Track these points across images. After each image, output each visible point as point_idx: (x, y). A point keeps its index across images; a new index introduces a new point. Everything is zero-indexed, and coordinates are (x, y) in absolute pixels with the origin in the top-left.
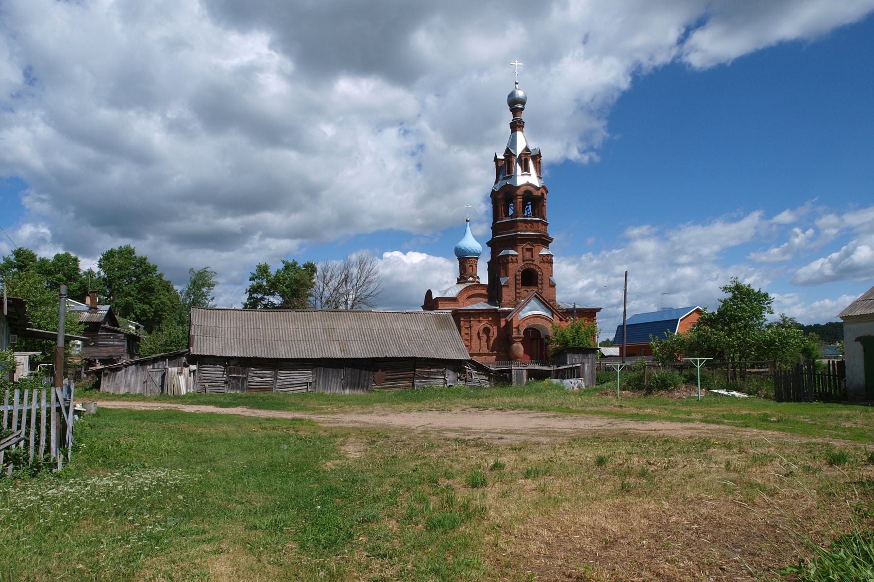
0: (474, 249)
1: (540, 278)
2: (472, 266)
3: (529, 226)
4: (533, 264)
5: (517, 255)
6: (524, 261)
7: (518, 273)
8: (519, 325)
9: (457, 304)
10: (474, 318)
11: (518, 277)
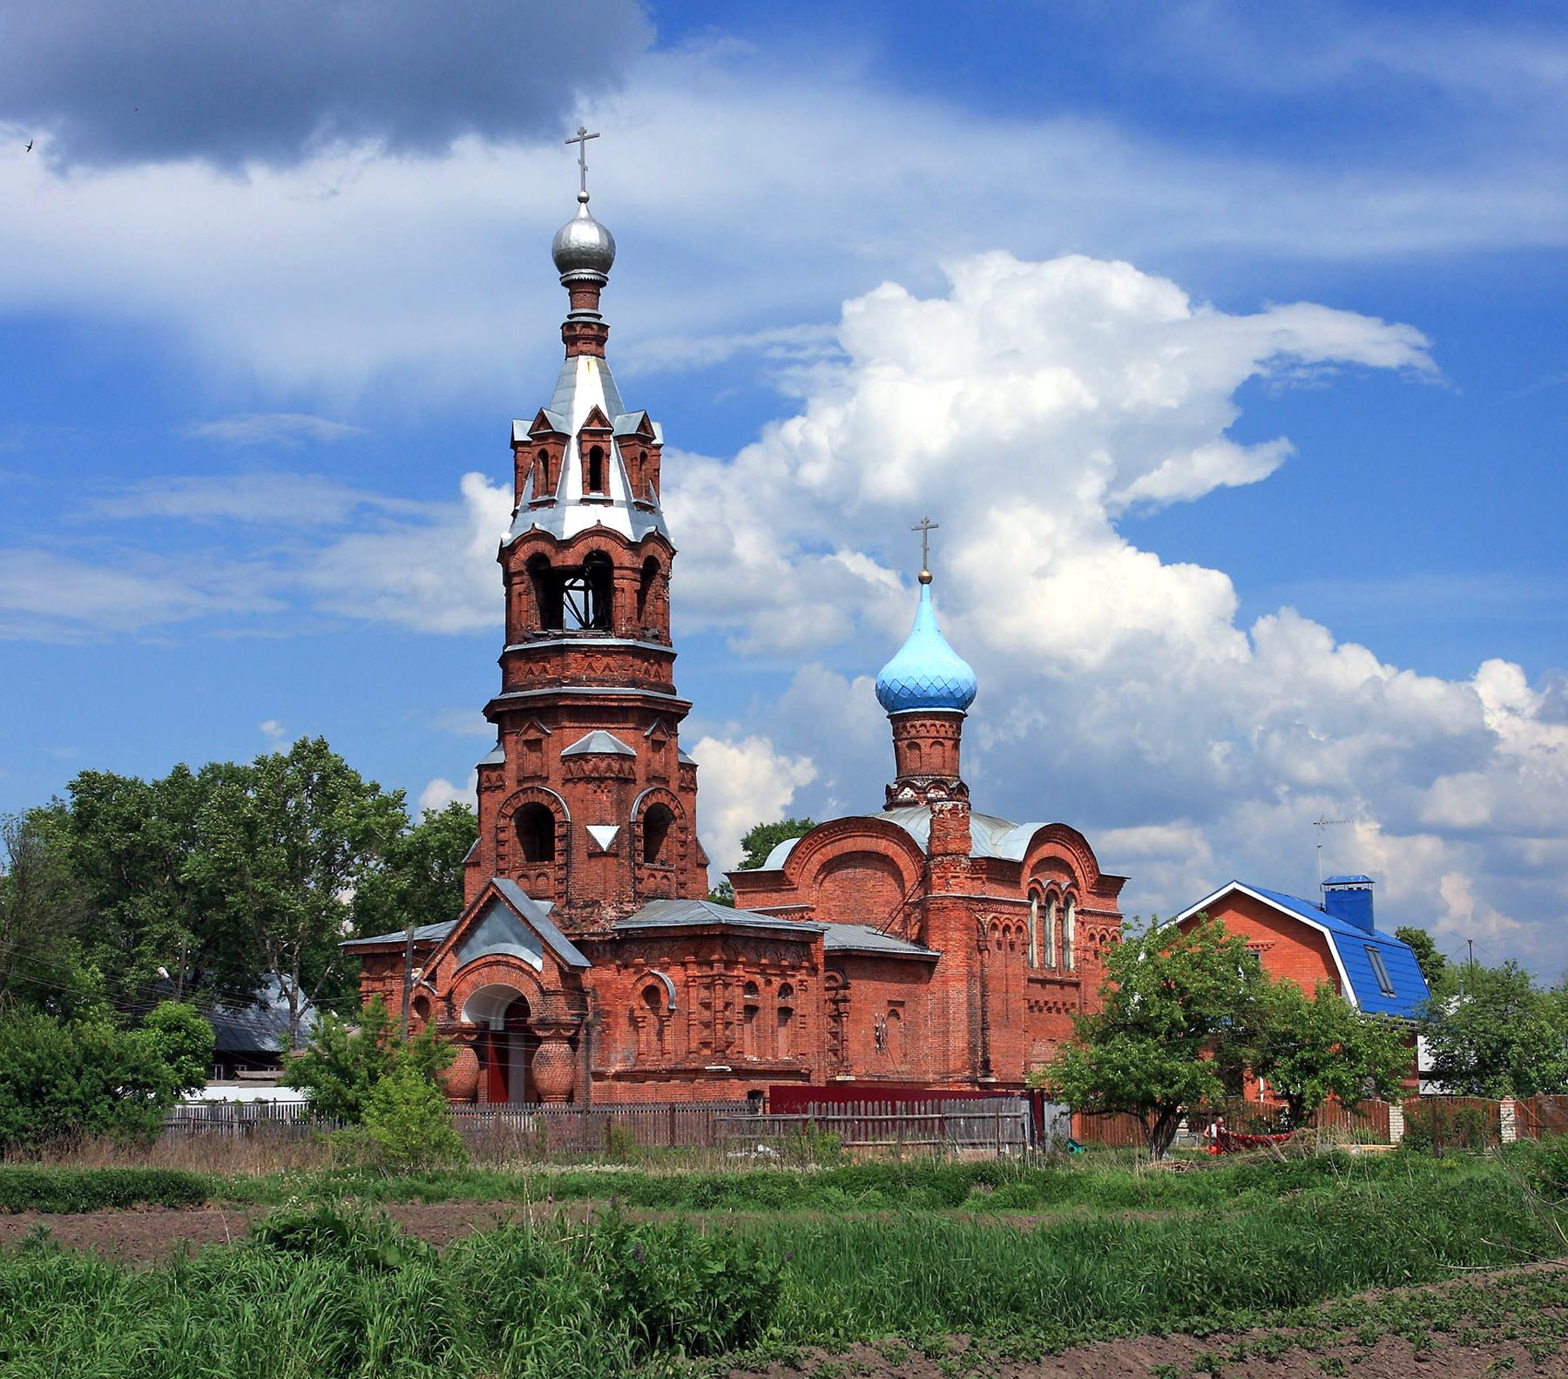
0: (910, 685)
1: (559, 831)
2: (918, 747)
3: (536, 668)
4: (541, 791)
5: (500, 766)
6: (520, 782)
7: (502, 822)
8: (451, 992)
9: (792, 895)
10: (392, 969)
11: (502, 836)
